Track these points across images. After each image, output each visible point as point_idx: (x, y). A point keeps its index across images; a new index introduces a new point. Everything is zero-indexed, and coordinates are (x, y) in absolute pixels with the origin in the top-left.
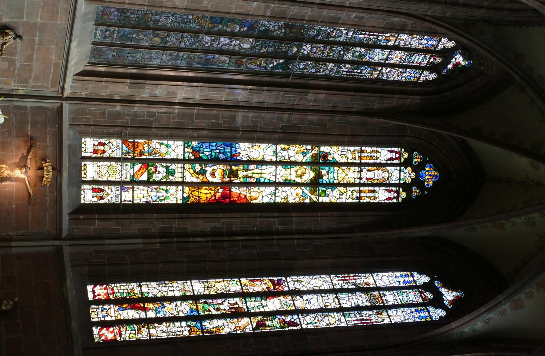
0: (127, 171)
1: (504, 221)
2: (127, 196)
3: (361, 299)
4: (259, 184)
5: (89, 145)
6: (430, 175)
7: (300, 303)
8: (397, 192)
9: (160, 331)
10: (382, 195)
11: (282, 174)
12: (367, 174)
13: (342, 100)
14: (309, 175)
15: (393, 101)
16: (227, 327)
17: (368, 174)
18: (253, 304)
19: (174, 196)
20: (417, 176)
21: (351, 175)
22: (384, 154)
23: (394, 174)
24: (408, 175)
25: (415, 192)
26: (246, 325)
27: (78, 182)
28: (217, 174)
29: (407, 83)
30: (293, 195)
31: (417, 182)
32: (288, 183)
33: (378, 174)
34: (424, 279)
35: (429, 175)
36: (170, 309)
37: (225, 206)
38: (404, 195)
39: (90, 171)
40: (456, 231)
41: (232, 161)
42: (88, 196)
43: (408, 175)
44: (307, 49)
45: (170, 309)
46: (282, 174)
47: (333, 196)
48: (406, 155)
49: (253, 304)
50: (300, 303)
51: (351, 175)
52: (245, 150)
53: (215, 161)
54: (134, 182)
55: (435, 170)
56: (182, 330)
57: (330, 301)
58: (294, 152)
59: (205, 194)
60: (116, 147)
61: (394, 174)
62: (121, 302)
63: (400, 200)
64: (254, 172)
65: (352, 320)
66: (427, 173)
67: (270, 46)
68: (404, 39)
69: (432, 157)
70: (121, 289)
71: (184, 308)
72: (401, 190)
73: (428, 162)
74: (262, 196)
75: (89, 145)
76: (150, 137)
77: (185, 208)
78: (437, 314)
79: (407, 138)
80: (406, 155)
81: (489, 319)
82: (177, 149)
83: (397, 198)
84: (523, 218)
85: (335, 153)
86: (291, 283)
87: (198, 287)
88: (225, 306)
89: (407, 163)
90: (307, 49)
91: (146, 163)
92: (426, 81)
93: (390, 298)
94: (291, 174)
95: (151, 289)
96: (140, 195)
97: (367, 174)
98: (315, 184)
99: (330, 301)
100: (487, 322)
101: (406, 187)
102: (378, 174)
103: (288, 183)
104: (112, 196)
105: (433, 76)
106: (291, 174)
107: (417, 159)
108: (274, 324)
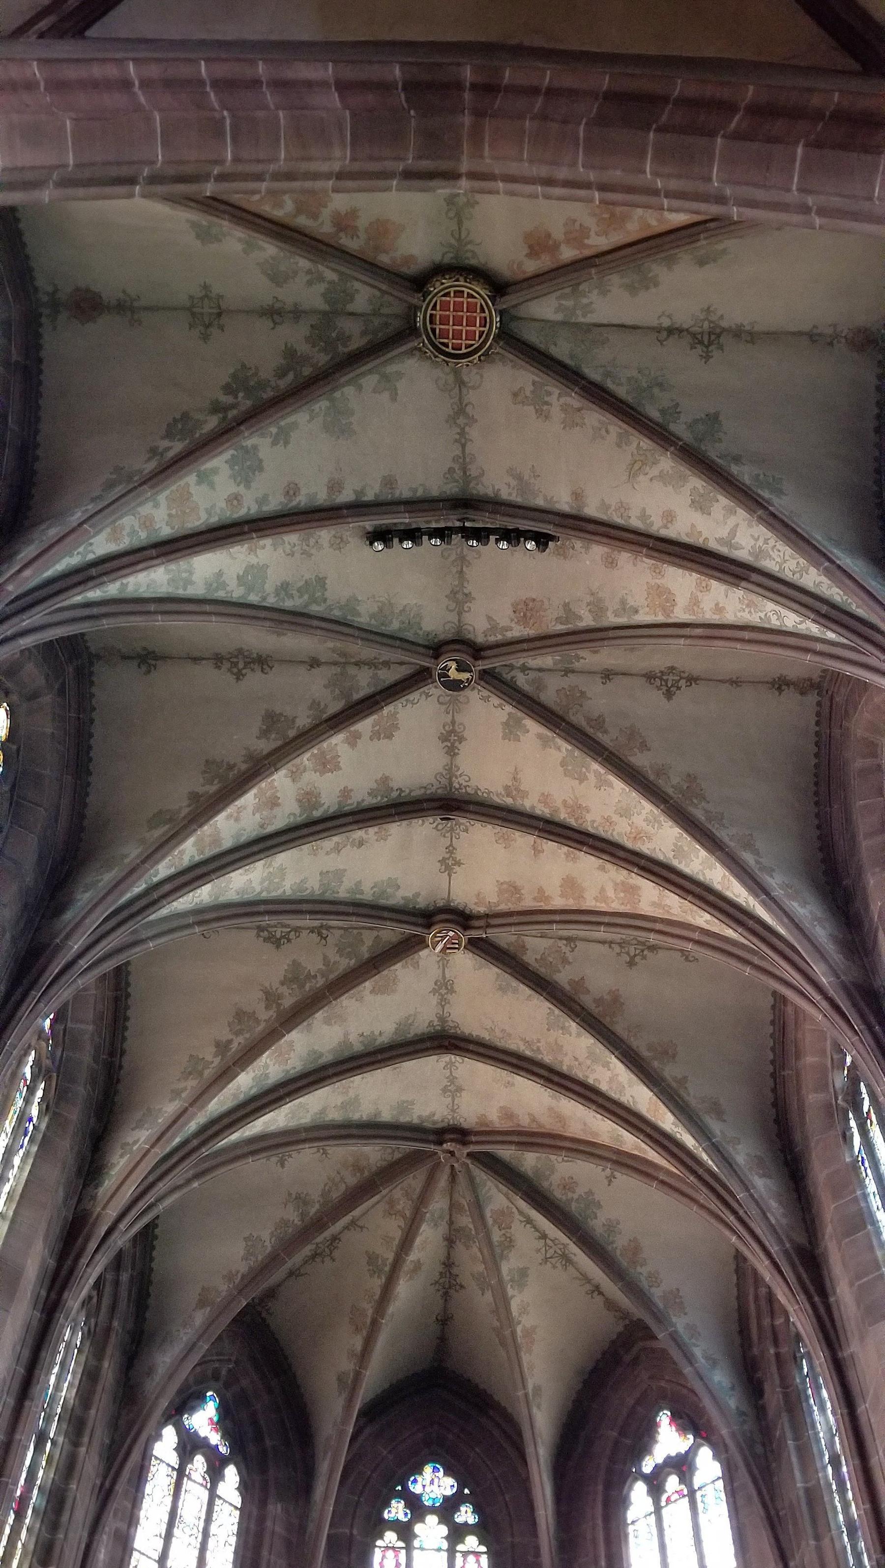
1: (519, 1329)
6: (432, 1482)
8: (465, 1554)
20: (433, 1510)
24: (430, 1531)
25: (466, 1515)
29: (243, 1532)
31: (446, 1509)
35: (434, 1483)
38: (471, 1542)
40: (541, 1424)
43: (430, 1531)
48: (390, 1537)
55: (420, 1472)
63: (483, 1549)
66: (428, 1489)
69: (394, 1479)
72: (460, 1547)
73: (405, 1488)
78: (708, 1467)
79: (355, 1532)
80: (390, 1537)
81: (707, 1358)
83: (477, 1554)
84: (510, 1292)
89: (405, 1532)
92: (244, 1488)
100: (714, 1363)
101: (457, 1533)
105: (231, 1474)
107: (397, 1510)
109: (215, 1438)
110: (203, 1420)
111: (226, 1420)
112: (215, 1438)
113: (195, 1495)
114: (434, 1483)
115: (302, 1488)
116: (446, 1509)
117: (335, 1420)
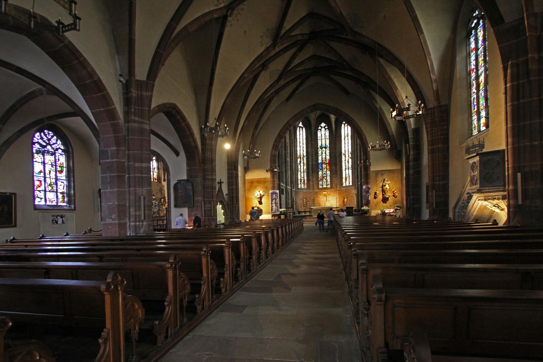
0: (324, 180)
2: (329, 180)
3: (346, 138)
4: (326, 158)
5: (320, 187)
7: (347, 150)
9: (351, 175)
10: (327, 134)
11: (324, 155)
12: (323, 138)
13: (310, 145)
14: (324, 149)
15: (309, 135)
16: (350, 164)
17: (323, 135)
18: (347, 159)
19: (328, 173)
21: (323, 141)
22: (319, 135)
23: (323, 132)
24: (323, 129)
25: (326, 127)
26: (350, 160)
27: (326, 188)
28: (324, 166)
30: (328, 152)
32: (325, 153)
33: (323, 136)
34: (343, 125)
35: (323, 125)
36: (347, 173)
37: (330, 163)
39: (325, 186)
41: (322, 163)
42: (329, 186)
43: (323, 129)
44: (302, 154)
45: (347, 173)
46: (324, 155)
47: (328, 144)
49: (347, 159)
50: (347, 150)
51: (323, 141)
52: (320, 161)
53: (322, 166)
54: (326, 179)
56: (350, 171)
57: (346, 144)
58: (320, 152)
59: (328, 167)
60: (320, 183)
61: (323, 132)
62: (346, 181)
64: (324, 159)
65: (350, 141)
67: (302, 160)
68: (298, 137)
70: (344, 181)
71: (347, 170)
74: (328, 157)
75: (320, 187)
76: (319, 177)
77: (330, 171)
82: (320, 173)
85: (319, 145)
86: (343, 152)
87: (344, 168)
88: (347, 164)
89: (321, 130)
90: (302, 154)
91: (323, 177)
93: (346, 133)
94: (324, 152)
95: (344, 176)
96: (328, 178)
97: (323, 138)
98: (326, 148)
99: (346, 144)
101: (326, 129)
102: (323, 136)
103: (325, 153)
104: (329, 183)
106: (324, 152)
107: (320, 128)
108: (350, 156)
109: (302, 126)
110: (301, 125)
111: (302, 124)
112: (302, 126)
113: (301, 131)
114: (323, 125)
115: (310, 128)
116: (325, 127)
117: (313, 122)
